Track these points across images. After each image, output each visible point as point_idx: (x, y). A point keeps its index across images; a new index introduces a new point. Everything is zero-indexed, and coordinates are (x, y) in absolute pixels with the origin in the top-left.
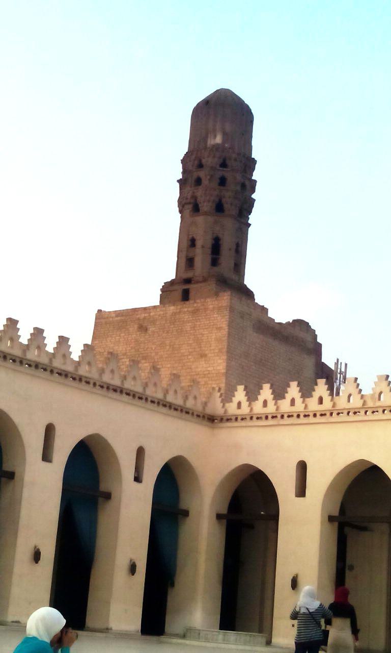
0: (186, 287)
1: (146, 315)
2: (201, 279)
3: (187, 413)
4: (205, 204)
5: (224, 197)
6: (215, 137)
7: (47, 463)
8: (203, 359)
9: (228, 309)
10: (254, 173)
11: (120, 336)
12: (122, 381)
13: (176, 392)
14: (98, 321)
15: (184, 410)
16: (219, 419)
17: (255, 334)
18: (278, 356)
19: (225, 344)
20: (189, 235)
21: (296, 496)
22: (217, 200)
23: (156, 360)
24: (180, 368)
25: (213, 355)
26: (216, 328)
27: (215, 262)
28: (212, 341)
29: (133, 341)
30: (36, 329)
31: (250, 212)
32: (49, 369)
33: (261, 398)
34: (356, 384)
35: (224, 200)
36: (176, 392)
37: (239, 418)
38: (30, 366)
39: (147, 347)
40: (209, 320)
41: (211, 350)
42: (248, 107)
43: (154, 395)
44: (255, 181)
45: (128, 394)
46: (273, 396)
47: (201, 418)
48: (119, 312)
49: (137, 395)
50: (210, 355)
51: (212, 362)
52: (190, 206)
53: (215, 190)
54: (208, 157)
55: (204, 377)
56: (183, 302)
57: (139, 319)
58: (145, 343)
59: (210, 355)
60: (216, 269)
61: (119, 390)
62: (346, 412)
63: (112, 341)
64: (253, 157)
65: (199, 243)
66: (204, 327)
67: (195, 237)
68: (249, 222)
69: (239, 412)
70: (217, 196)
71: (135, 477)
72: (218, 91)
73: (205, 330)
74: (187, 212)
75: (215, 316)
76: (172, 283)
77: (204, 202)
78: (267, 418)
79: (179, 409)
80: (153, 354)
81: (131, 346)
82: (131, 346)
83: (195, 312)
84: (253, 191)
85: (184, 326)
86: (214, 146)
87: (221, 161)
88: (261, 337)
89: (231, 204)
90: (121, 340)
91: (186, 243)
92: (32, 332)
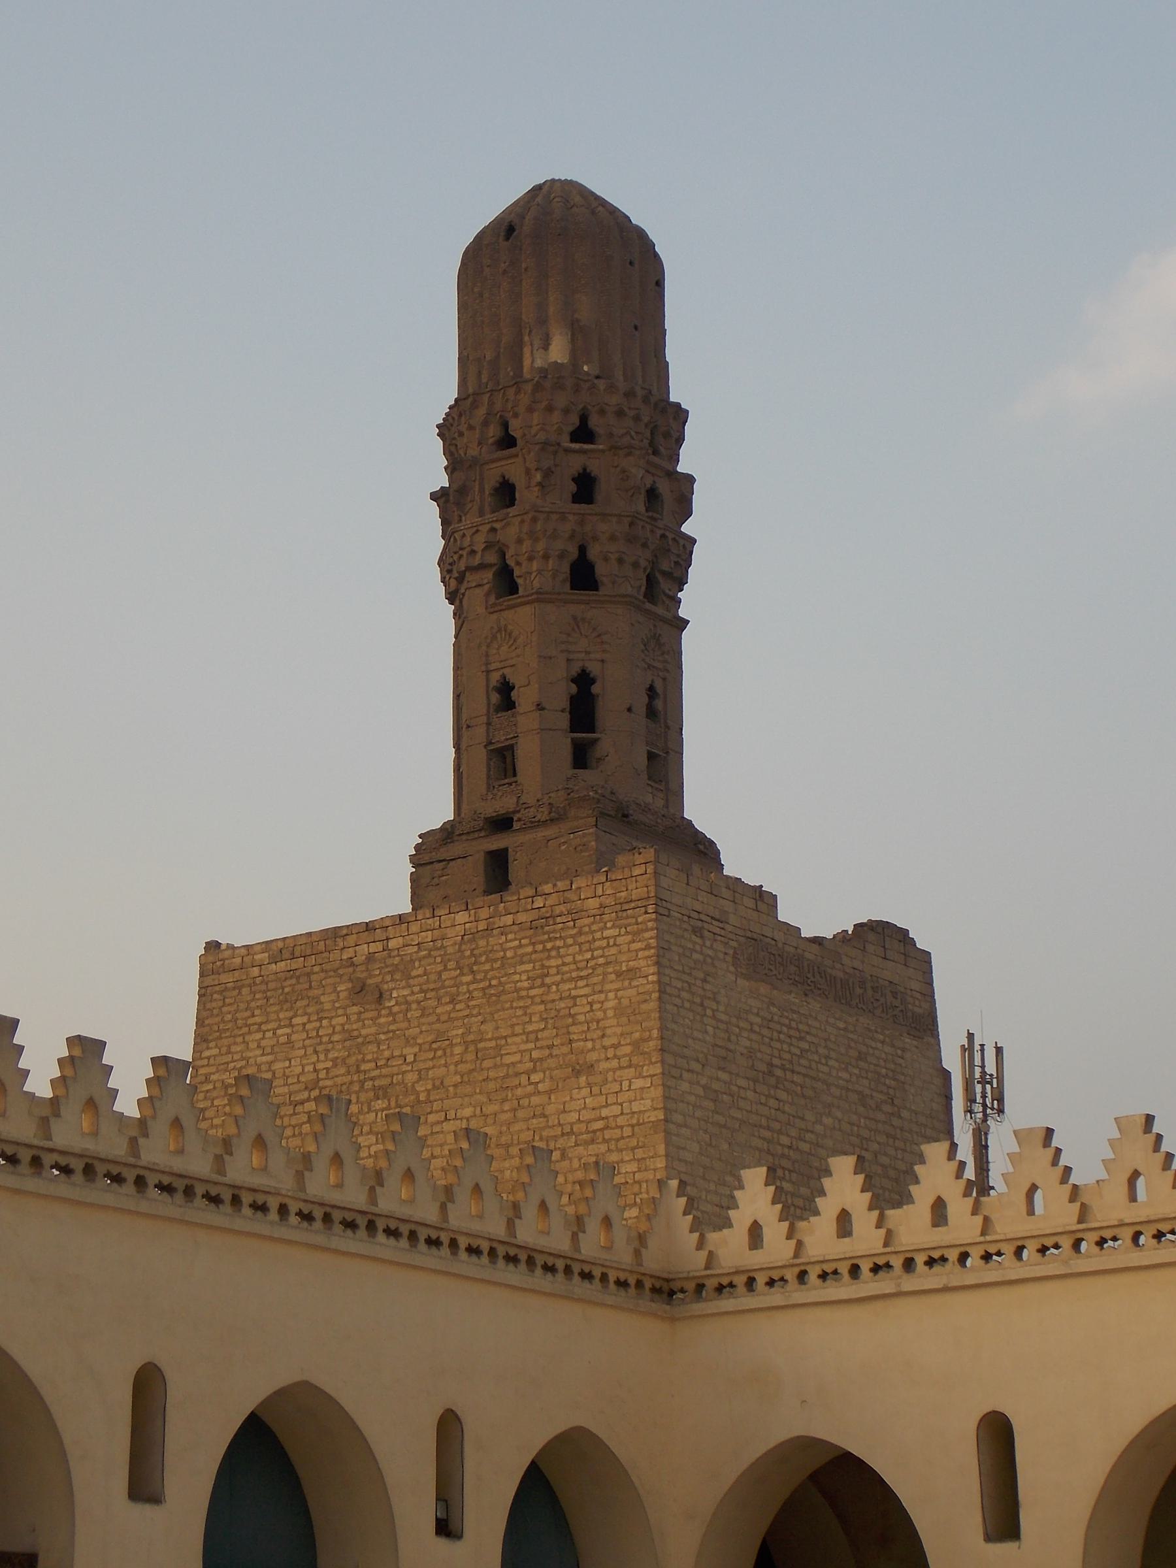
0: (497, 842)
1: (373, 948)
2: (543, 815)
3: (586, 1276)
4: (535, 566)
5: (595, 538)
6: (546, 347)
7: (147, 1509)
8: (583, 1079)
9: (651, 909)
10: (684, 451)
11: (291, 1025)
12: (372, 1189)
13: (543, 1206)
14: (209, 981)
15: (576, 1268)
16: (690, 1286)
17: (739, 981)
18: (821, 1051)
19: (654, 1023)
20: (488, 672)
21: (988, 1538)
22: (574, 553)
23: (422, 1097)
24: (509, 1115)
25: (615, 1063)
26: (619, 974)
27: (581, 757)
28: (605, 1018)
29: (336, 1038)
30: (76, 1041)
31: (681, 582)
32: (130, 1175)
33: (828, 1207)
34: (1151, 1138)
35: (593, 553)
36: (543, 1206)
37: (761, 1279)
38: (66, 1170)
39: (387, 1054)
40: (591, 950)
41: (604, 1047)
42: (641, 234)
43: (476, 1226)
44: (690, 480)
45: (392, 1233)
46: (868, 1196)
47: (632, 1290)
48: (280, 945)
49: (423, 1234)
50: (604, 1065)
51: (616, 1088)
52: (489, 575)
53: (563, 517)
54: (530, 410)
55: (593, 1141)
56: (495, 897)
57: (351, 963)
58: (379, 1044)
59: (604, 1065)
60: (588, 776)
61: (362, 1222)
62: (1127, 1233)
63: (263, 1043)
64: (673, 398)
65: (525, 698)
66: (574, 974)
67: (512, 679)
68: (682, 613)
69: (756, 1259)
70: (572, 537)
71: (437, 1519)
72: (537, 189)
73: (581, 983)
74: (476, 599)
75: (607, 933)
76: (447, 834)
77: (531, 559)
78: (855, 1271)
79: (560, 1264)
80: (411, 1077)
81: (330, 1056)
82: (330, 1056)
83: (541, 924)
84: (689, 513)
85: (506, 975)
86: (544, 373)
87: (575, 420)
88: (764, 989)
89: (620, 561)
90: (294, 1037)
91: (480, 703)
92: (65, 1053)
